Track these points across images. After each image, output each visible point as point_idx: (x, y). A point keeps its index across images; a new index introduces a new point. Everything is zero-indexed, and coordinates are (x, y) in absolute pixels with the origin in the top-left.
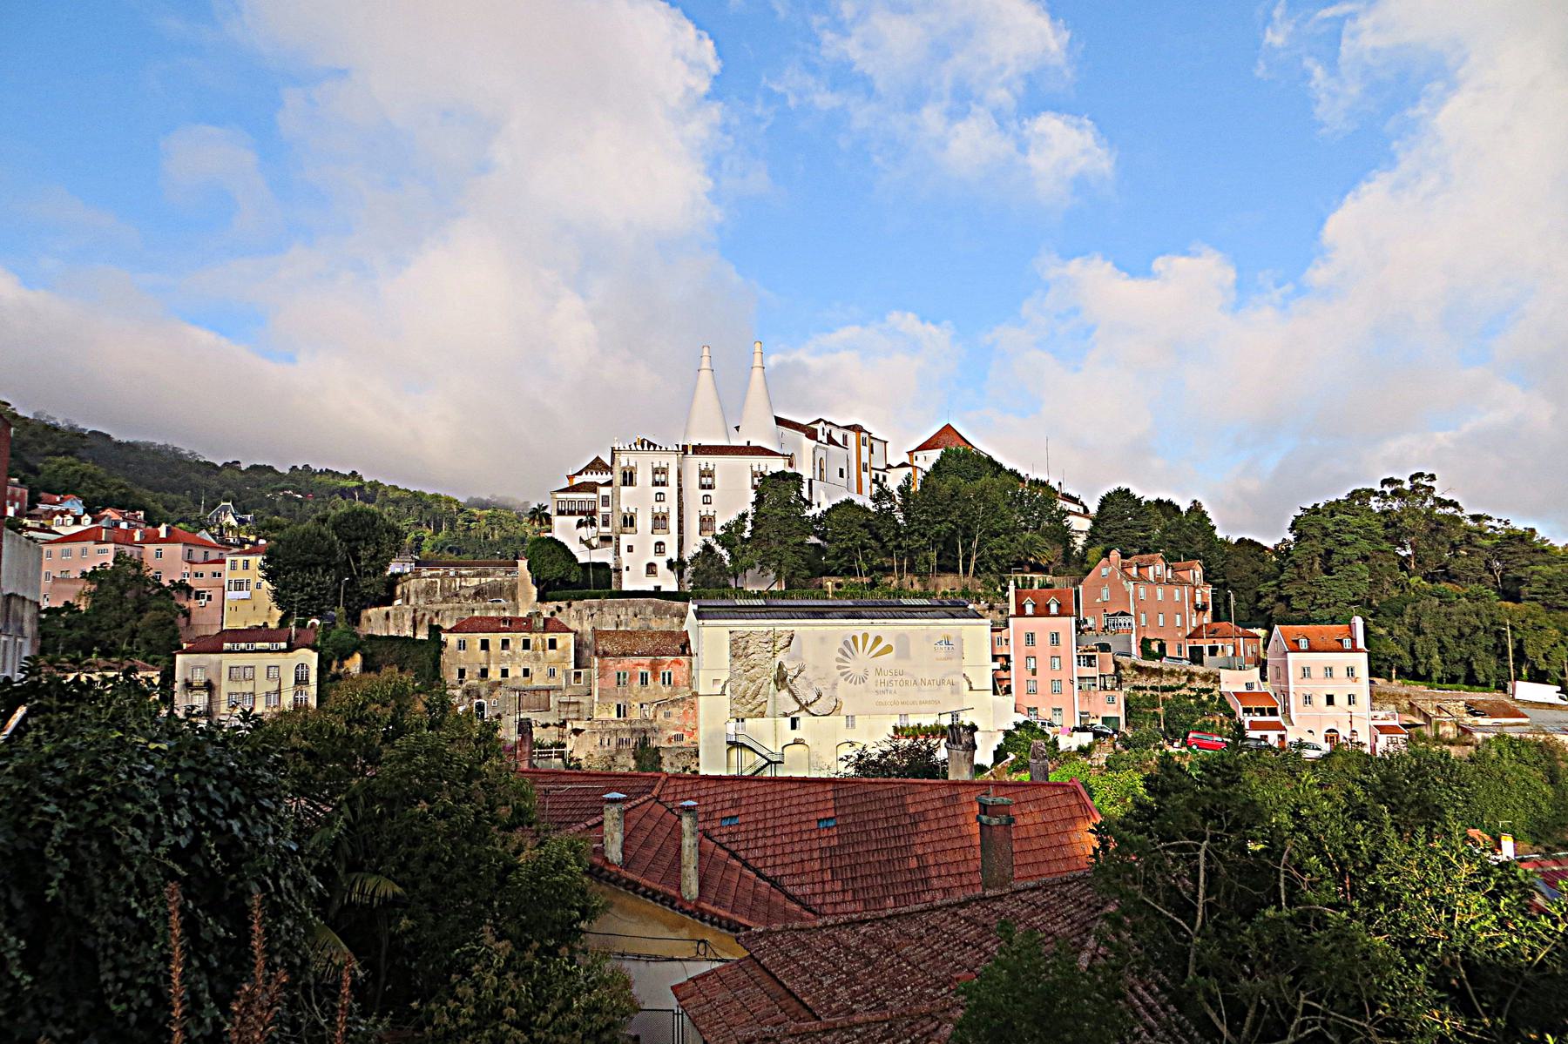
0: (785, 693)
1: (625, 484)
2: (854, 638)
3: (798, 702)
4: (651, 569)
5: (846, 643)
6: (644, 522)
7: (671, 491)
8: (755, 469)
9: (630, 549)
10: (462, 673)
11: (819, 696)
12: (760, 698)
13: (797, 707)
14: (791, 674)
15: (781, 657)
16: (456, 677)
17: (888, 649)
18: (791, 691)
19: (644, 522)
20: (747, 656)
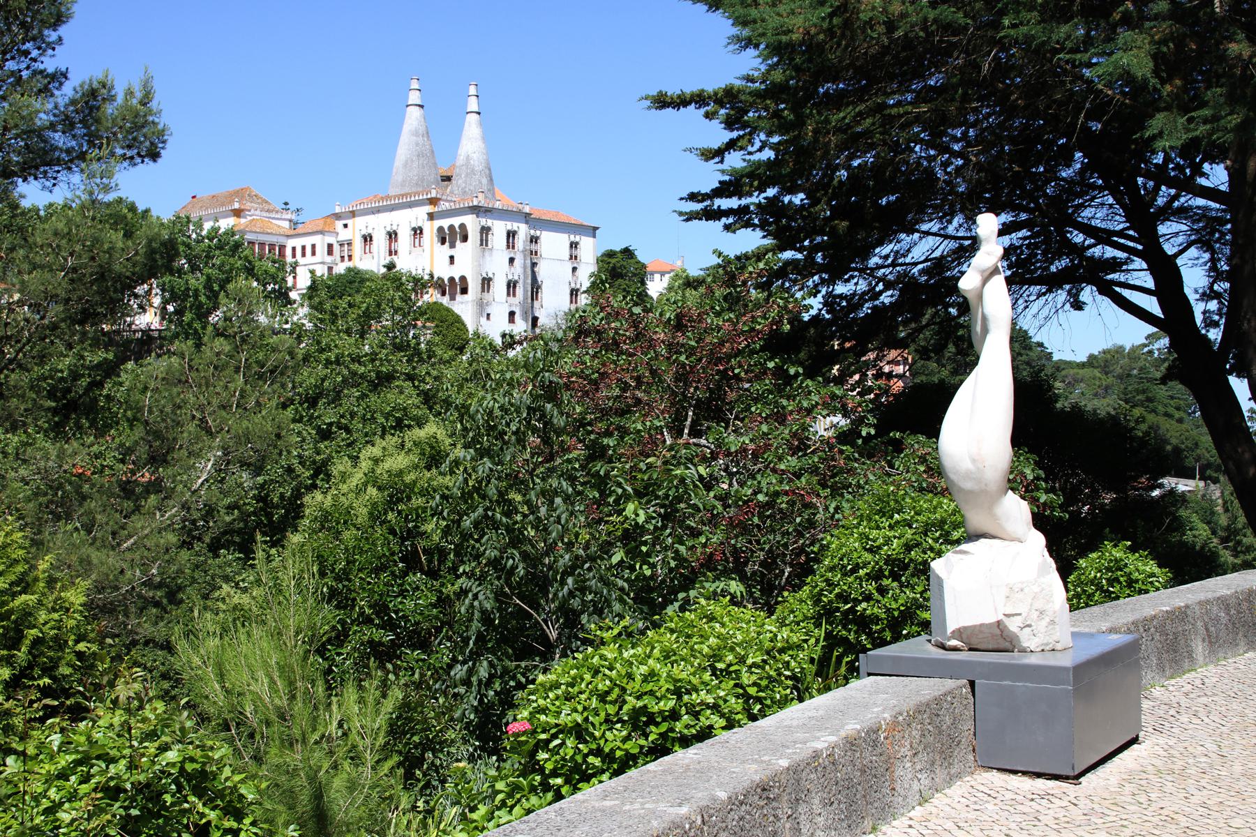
6: (499, 287)
19: (499, 287)
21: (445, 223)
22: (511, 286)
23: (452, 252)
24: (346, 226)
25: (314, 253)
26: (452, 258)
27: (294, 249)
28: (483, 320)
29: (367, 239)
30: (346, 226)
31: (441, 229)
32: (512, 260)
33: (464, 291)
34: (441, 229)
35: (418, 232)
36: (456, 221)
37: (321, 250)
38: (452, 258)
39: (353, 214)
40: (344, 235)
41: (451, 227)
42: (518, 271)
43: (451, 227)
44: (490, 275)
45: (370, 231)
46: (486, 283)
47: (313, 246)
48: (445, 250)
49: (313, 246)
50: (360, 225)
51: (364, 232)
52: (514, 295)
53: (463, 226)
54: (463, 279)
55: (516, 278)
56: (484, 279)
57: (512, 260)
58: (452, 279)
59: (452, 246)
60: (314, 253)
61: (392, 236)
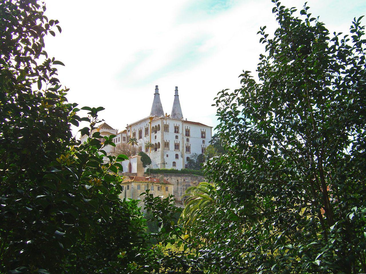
4: (174, 163)
6: (172, 146)
8: (202, 131)
9: (167, 156)
19: (172, 146)
21: (154, 125)
23: (156, 134)
24: (129, 131)
26: (156, 136)
28: (165, 157)
29: (134, 134)
31: (153, 127)
32: (177, 137)
34: (153, 127)
35: (147, 130)
41: (156, 126)
43: (156, 126)
45: (135, 131)
46: (167, 145)
47: (119, 138)
48: (153, 135)
49: (119, 138)
51: (133, 132)
53: (159, 125)
54: (159, 143)
55: (178, 143)
57: (177, 137)
58: (156, 144)
59: (156, 133)
60: (119, 141)
61: (140, 132)
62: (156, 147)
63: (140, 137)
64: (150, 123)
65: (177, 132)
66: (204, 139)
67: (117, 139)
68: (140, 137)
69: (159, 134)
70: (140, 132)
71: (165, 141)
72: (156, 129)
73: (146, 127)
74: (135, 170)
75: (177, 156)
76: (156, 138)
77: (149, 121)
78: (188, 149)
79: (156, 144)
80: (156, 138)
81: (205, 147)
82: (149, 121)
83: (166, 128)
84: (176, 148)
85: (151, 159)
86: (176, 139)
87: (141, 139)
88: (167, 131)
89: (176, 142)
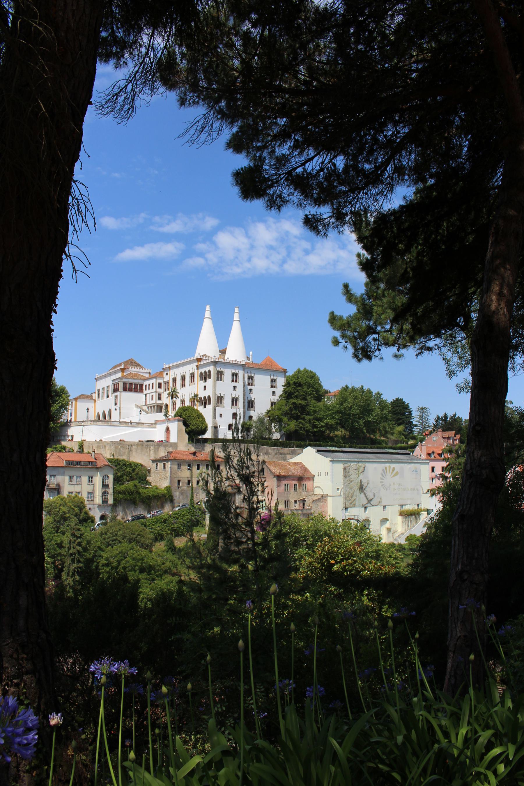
0: (362, 494)
1: (218, 380)
2: (386, 468)
3: (367, 499)
5: (383, 470)
6: (227, 401)
7: (240, 385)
9: (221, 415)
10: (179, 482)
11: (374, 496)
12: (354, 497)
13: (367, 502)
14: (365, 485)
15: (361, 477)
16: (176, 485)
17: (397, 473)
18: (365, 494)
19: (227, 401)
20: (349, 476)
21: (203, 370)
22: (235, 401)
23: (205, 384)
24: (167, 374)
25: (153, 388)
26: (205, 387)
27: (146, 386)
29: (174, 380)
30: (167, 374)
31: (201, 373)
32: (235, 387)
33: (210, 403)
34: (201, 373)
35: (192, 375)
36: (207, 369)
37: (156, 386)
38: (205, 387)
39: (170, 368)
40: (166, 378)
41: (205, 372)
42: (239, 393)
43: (205, 372)
44: (222, 395)
46: (220, 399)
47: (153, 384)
48: (202, 383)
49: (153, 384)
50: (173, 373)
52: (236, 405)
53: (209, 371)
54: (209, 397)
55: (237, 396)
56: (218, 397)
57: (235, 387)
58: (205, 397)
59: (205, 381)
60: (153, 388)
61: (183, 378)
62: (205, 402)
63: (183, 385)
64: (197, 366)
65: (236, 381)
66: (273, 389)
67: (149, 385)
68: (183, 385)
69: (210, 382)
70: (183, 378)
71: (219, 395)
72: (205, 377)
73: (191, 372)
74: (173, 439)
75: (235, 415)
76: (205, 389)
77: (196, 364)
78: (250, 404)
79: (205, 397)
80: (205, 389)
81: (276, 401)
82: (196, 364)
83: (220, 375)
84: (233, 404)
85: (200, 412)
86: (235, 392)
87: (184, 388)
88: (221, 380)
89: (234, 396)
